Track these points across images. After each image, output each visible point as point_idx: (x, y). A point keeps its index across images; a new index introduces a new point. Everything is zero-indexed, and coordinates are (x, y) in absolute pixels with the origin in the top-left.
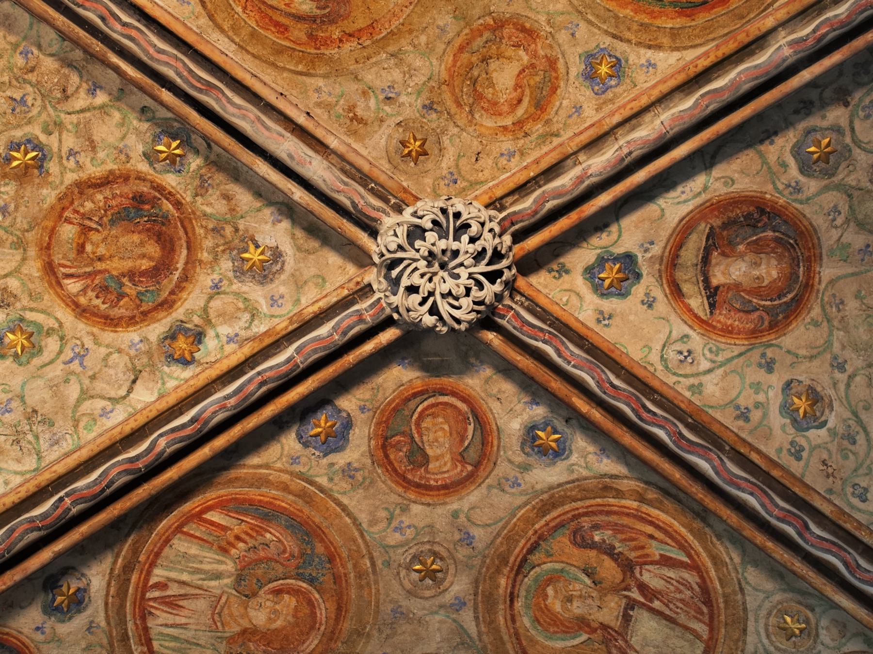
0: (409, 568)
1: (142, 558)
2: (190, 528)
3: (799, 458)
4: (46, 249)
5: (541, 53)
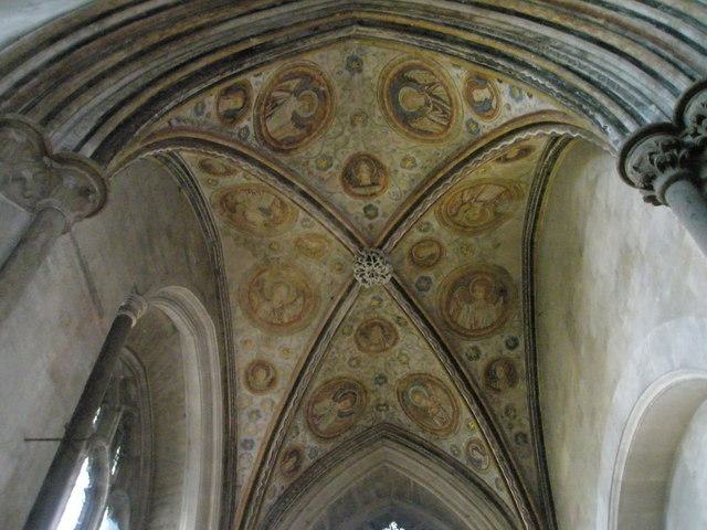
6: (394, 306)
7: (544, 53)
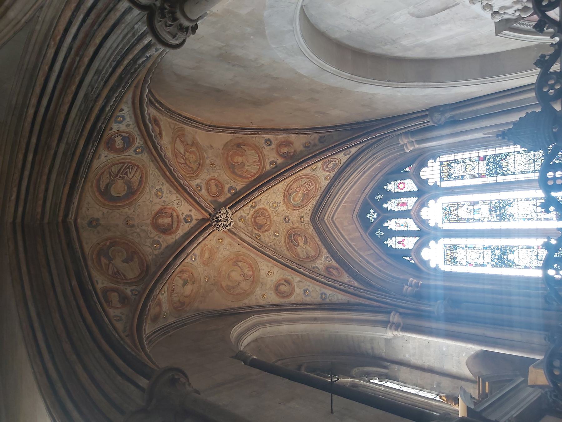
3: (163, 183)
4: (271, 220)
6: (245, 208)
7: (95, 96)
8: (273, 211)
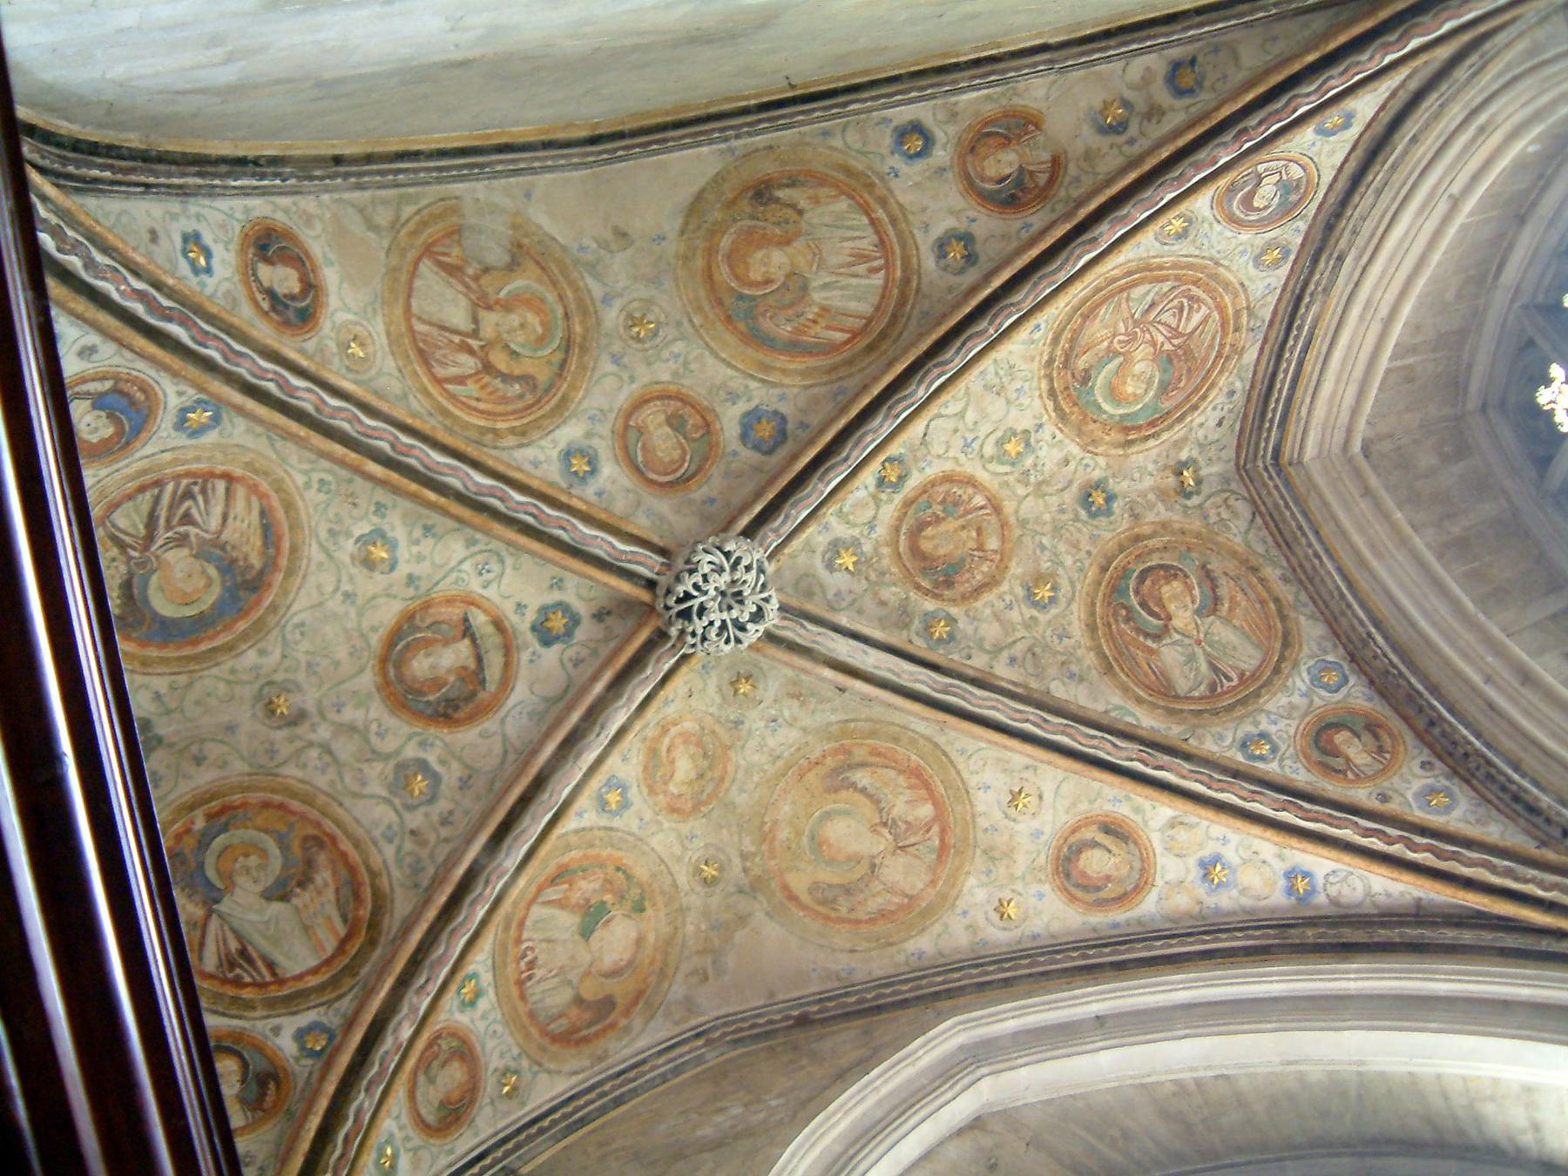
0: (659, 323)
1: (896, 291)
2: (858, 324)
3: (378, 503)
4: (1004, 525)
5: (661, 797)
8: (1011, 478)
